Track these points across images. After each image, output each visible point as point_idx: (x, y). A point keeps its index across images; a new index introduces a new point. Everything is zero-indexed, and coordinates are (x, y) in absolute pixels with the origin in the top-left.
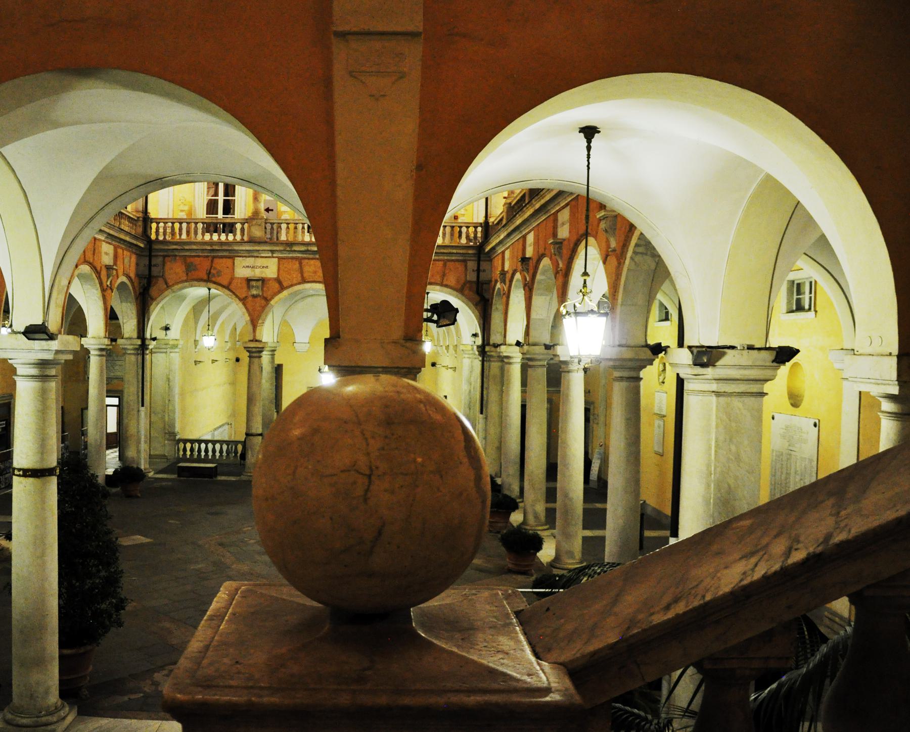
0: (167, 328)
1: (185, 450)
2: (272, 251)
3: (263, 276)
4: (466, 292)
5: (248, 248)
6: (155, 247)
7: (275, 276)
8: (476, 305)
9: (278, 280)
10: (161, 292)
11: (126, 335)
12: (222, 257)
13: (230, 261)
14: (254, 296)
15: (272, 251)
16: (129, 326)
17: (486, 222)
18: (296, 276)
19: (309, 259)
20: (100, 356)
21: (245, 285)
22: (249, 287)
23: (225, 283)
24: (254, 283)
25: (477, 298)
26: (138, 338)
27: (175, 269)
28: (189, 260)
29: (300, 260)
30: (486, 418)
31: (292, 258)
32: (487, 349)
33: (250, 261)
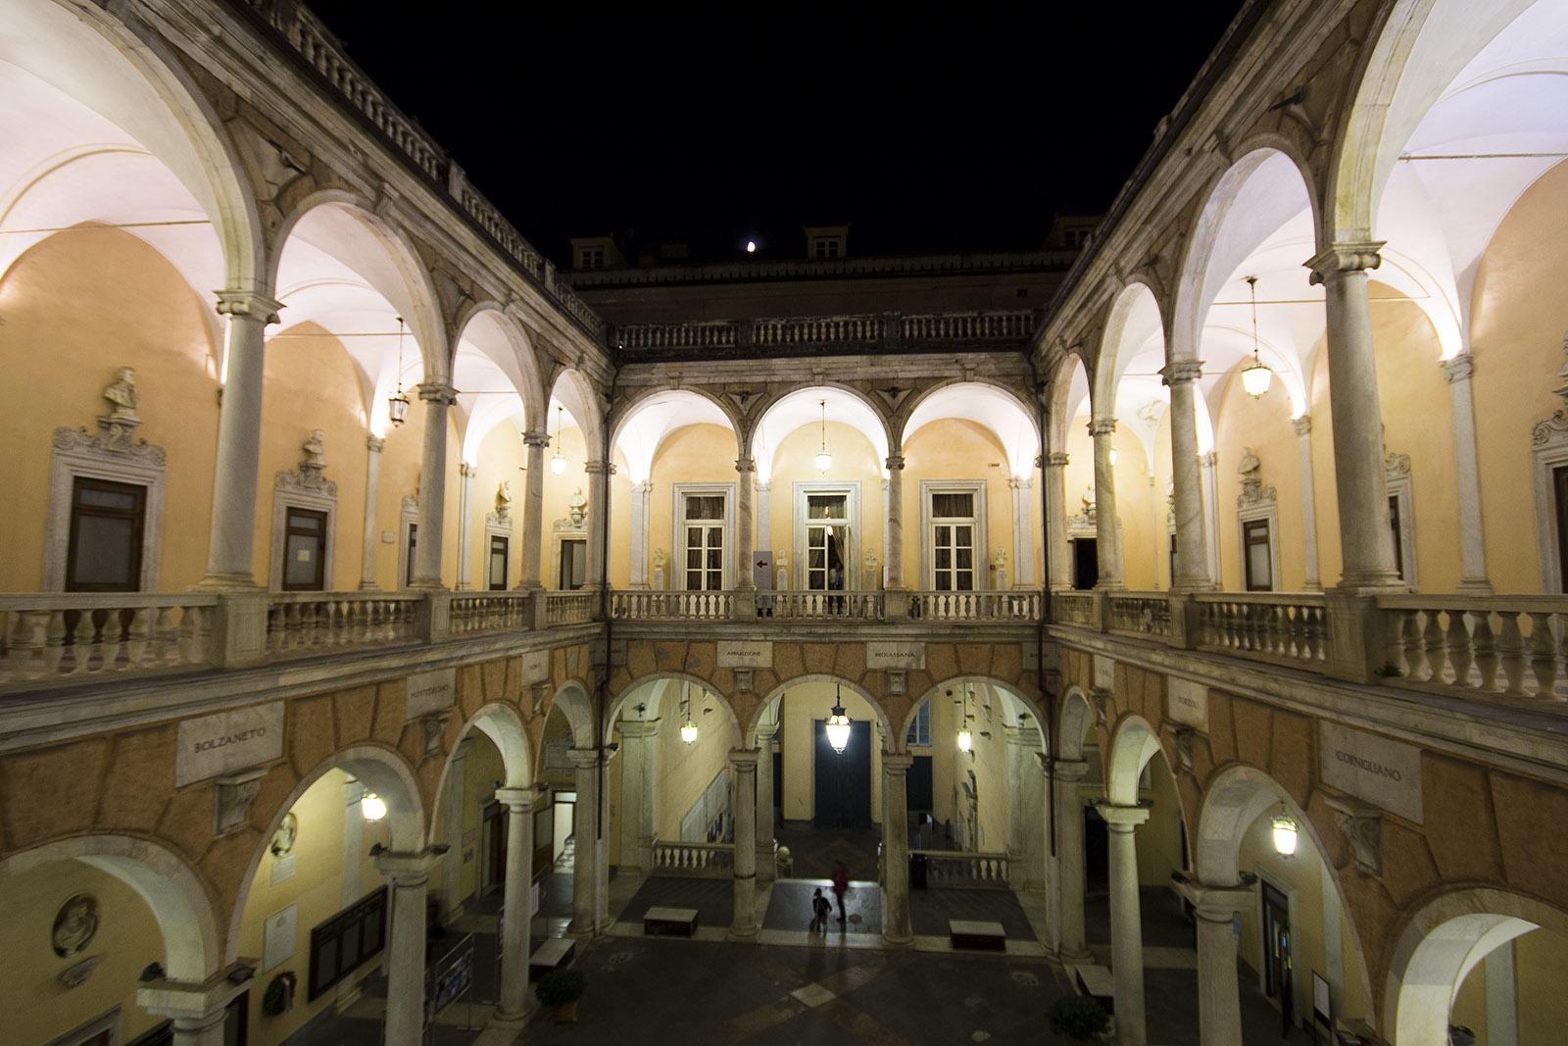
0: (641, 709)
1: (663, 857)
2: (765, 635)
3: (754, 664)
5: (733, 630)
6: (615, 629)
7: (770, 665)
8: (1037, 702)
9: (773, 671)
10: (624, 686)
11: (579, 744)
12: (700, 642)
13: (710, 646)
14: (743, 693)
15: (765, 635)
16: (583, 734)
17: (1047, 592)
19: (813, 643)
20: (522, 813)
21: (730, 678)
23: (706, 675)
24: (741, 676)
25: (1038, 693)
26: (594, 748)
27: (641, 656)
28: (658, 644)
29: (801, 645)
30: (1060, 860)
31: (792, 642)
32: (1057, 765)
33: (737, 646)
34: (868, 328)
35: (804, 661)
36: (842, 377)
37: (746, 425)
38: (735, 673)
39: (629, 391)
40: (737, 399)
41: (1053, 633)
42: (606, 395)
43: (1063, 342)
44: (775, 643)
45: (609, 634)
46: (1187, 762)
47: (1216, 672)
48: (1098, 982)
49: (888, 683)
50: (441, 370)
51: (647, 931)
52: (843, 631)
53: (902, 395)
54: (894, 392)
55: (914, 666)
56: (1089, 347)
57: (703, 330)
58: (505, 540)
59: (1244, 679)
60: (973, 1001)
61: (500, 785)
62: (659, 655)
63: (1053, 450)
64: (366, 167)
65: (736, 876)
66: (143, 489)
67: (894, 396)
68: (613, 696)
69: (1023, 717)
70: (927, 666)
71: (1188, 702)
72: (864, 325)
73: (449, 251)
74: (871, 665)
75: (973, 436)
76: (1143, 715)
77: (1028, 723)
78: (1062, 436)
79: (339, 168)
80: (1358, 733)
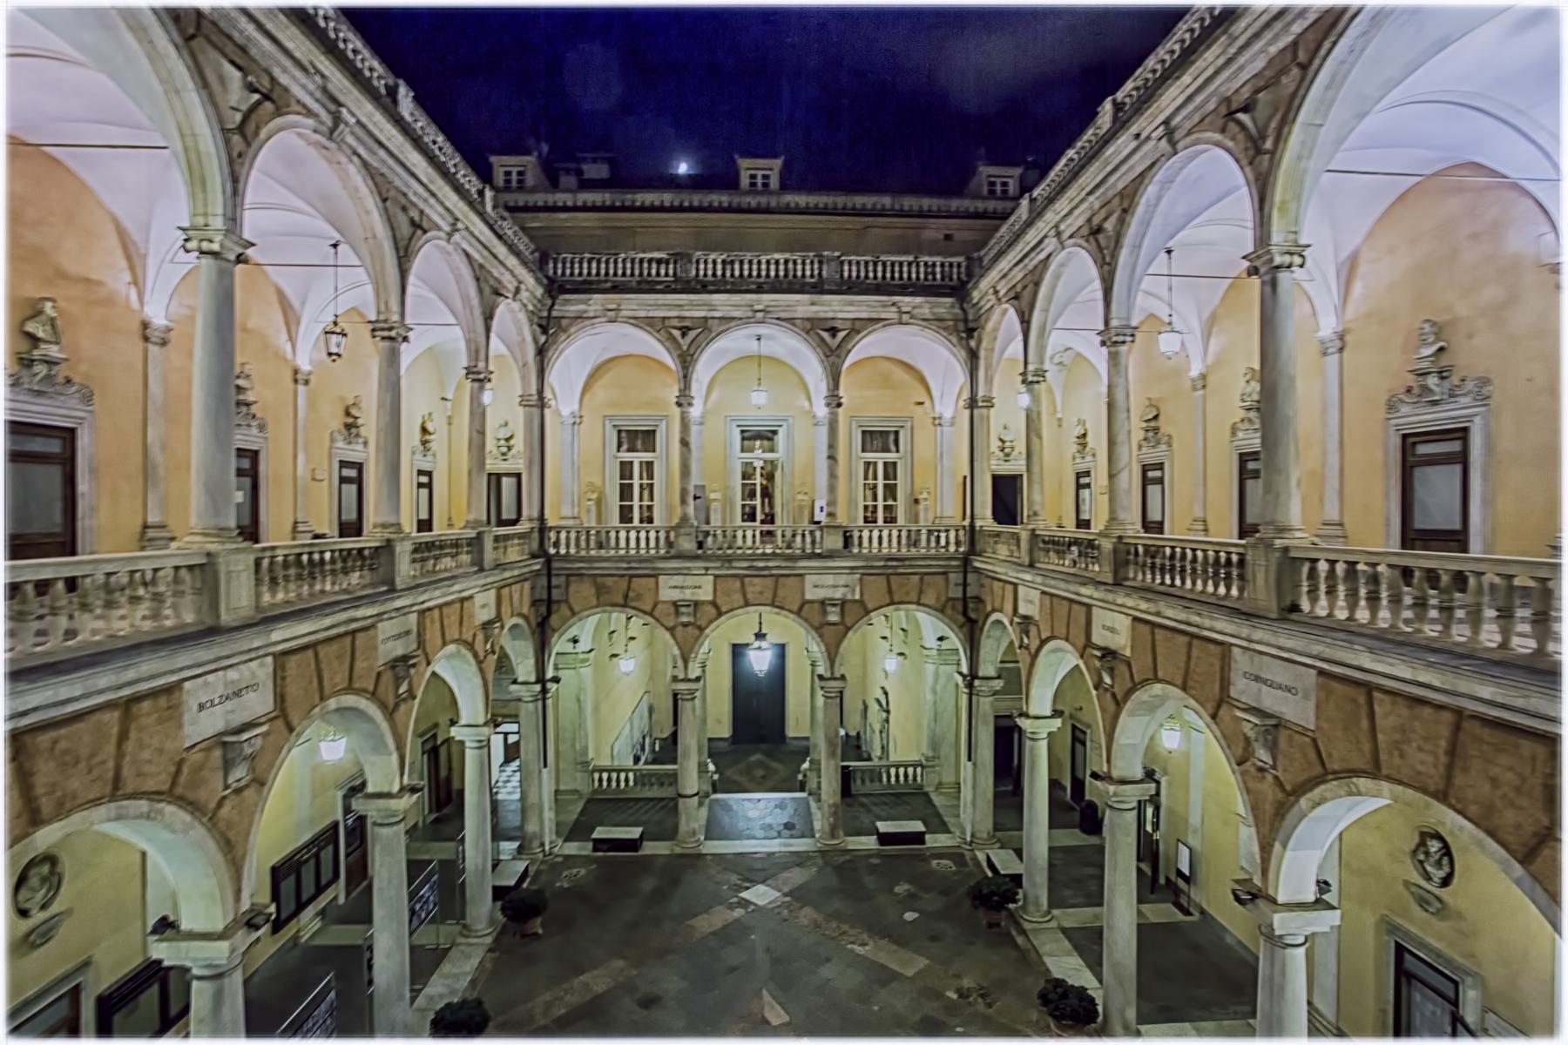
4: (949, 611)
6: (555, 565)
7: (710, 598)
8: (961, 627)
10: (564, 621)
13: (652, 580)
14: (685, 625)
15: (707, 569)
16: (525, 668)
18: (737, 598)
21: (672, 610)
22: (677, 613)
23: (648, 608)
24: (683, 610)
25: (961, 619)
27: (582, 592)
28: (599, 580)
32: (977, 683)
34: (808, 267)
35: (744, 594)
36: (783, 315)
37: (686, 361)
38: (676, 605)
39: (564, 322)
40: (677, 333)
41: (977, 564)
42: (540, 326)
43: (996, 292)
44: (716, 577)
45: (549, 569)
46: (1107, 680)
47: (1144, 606)
48: (1006, 862)
49: (825, 613)
50: (394, 306)
51: (595, 849)
52: (784, 564)
53: (841, 335)
54: (833, 331)
55: (849, 597)
56: (1024, 300)
57: (641, 261)
58: (429, 474)
59: (1169, 613)
60: (901, 889)
61: (453, 723)
62: (600, 591)
63: (981, 394)
64: (325, 90)
65: (680, 796)
66: (72, 431)
67: (834, 336)
68: (554, 631)
69: (941, 639)
70: (862, 594)
71: (1112, 630)
72: (804, 263)
73: (400, 179)
74: (808, 597)
75: (900, 374)
76: (1067, 640)
77: (945, 645)
78: (989, 381)
79: (297, 91)
80: (1265, 658)
